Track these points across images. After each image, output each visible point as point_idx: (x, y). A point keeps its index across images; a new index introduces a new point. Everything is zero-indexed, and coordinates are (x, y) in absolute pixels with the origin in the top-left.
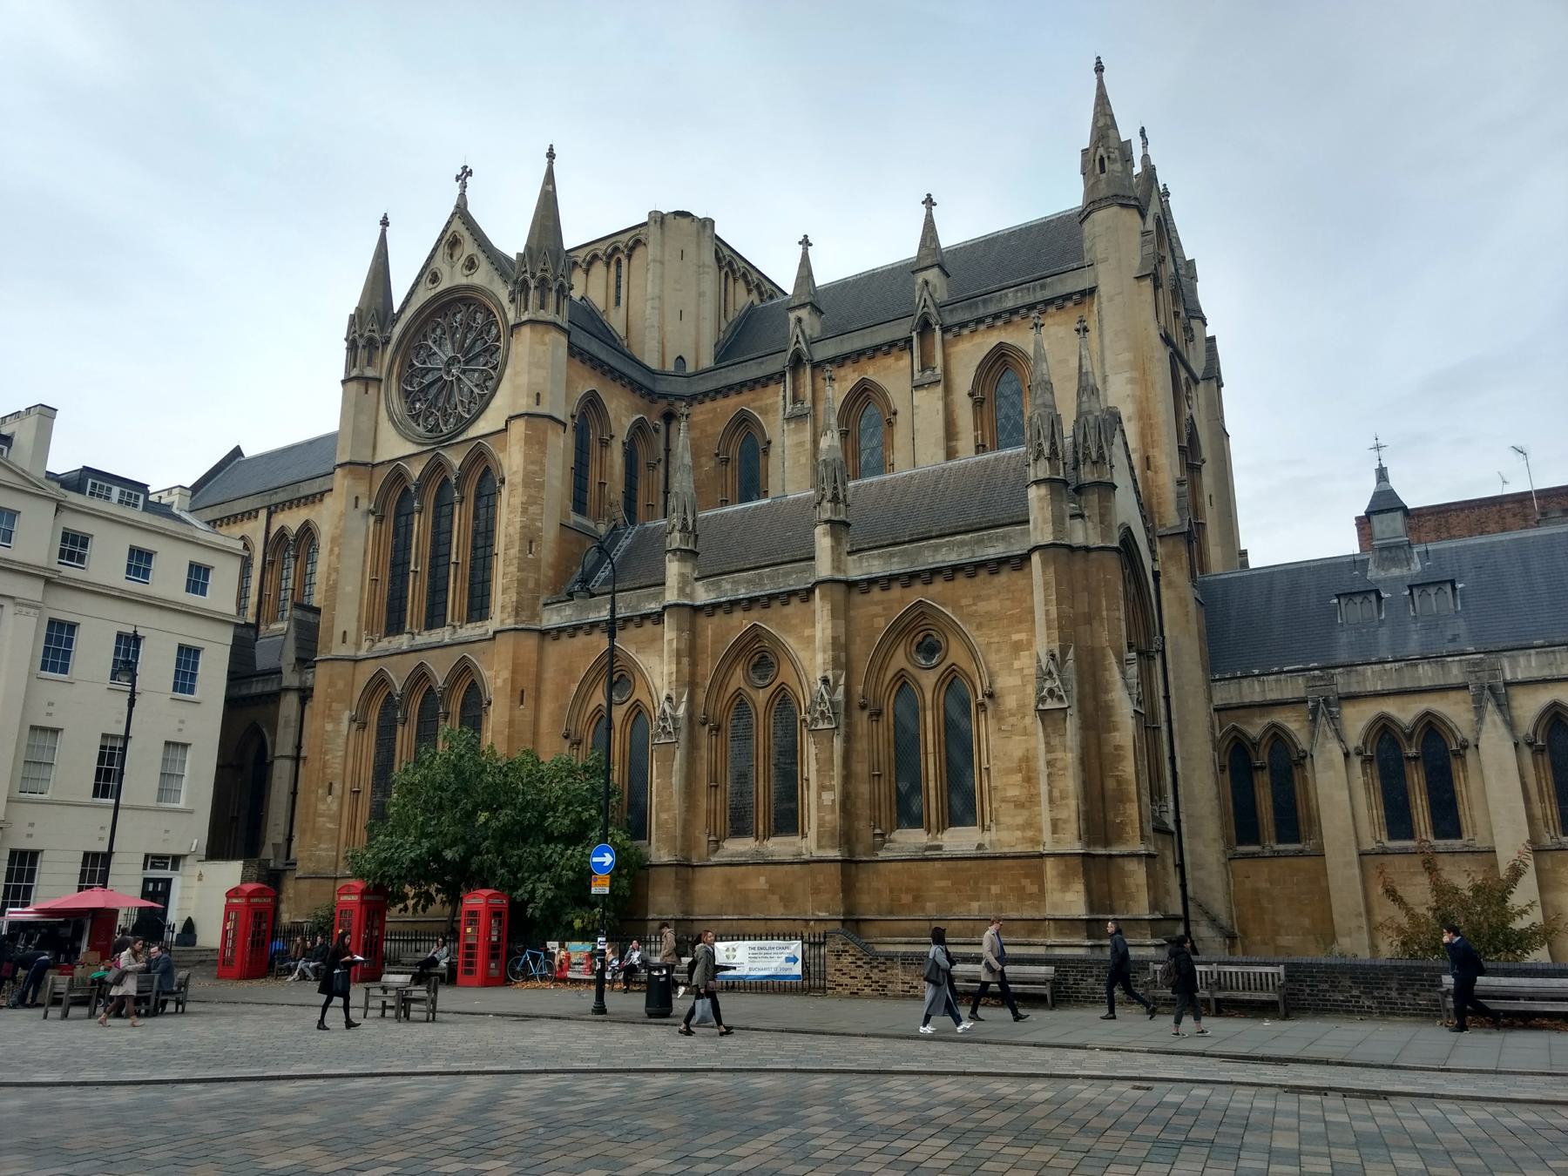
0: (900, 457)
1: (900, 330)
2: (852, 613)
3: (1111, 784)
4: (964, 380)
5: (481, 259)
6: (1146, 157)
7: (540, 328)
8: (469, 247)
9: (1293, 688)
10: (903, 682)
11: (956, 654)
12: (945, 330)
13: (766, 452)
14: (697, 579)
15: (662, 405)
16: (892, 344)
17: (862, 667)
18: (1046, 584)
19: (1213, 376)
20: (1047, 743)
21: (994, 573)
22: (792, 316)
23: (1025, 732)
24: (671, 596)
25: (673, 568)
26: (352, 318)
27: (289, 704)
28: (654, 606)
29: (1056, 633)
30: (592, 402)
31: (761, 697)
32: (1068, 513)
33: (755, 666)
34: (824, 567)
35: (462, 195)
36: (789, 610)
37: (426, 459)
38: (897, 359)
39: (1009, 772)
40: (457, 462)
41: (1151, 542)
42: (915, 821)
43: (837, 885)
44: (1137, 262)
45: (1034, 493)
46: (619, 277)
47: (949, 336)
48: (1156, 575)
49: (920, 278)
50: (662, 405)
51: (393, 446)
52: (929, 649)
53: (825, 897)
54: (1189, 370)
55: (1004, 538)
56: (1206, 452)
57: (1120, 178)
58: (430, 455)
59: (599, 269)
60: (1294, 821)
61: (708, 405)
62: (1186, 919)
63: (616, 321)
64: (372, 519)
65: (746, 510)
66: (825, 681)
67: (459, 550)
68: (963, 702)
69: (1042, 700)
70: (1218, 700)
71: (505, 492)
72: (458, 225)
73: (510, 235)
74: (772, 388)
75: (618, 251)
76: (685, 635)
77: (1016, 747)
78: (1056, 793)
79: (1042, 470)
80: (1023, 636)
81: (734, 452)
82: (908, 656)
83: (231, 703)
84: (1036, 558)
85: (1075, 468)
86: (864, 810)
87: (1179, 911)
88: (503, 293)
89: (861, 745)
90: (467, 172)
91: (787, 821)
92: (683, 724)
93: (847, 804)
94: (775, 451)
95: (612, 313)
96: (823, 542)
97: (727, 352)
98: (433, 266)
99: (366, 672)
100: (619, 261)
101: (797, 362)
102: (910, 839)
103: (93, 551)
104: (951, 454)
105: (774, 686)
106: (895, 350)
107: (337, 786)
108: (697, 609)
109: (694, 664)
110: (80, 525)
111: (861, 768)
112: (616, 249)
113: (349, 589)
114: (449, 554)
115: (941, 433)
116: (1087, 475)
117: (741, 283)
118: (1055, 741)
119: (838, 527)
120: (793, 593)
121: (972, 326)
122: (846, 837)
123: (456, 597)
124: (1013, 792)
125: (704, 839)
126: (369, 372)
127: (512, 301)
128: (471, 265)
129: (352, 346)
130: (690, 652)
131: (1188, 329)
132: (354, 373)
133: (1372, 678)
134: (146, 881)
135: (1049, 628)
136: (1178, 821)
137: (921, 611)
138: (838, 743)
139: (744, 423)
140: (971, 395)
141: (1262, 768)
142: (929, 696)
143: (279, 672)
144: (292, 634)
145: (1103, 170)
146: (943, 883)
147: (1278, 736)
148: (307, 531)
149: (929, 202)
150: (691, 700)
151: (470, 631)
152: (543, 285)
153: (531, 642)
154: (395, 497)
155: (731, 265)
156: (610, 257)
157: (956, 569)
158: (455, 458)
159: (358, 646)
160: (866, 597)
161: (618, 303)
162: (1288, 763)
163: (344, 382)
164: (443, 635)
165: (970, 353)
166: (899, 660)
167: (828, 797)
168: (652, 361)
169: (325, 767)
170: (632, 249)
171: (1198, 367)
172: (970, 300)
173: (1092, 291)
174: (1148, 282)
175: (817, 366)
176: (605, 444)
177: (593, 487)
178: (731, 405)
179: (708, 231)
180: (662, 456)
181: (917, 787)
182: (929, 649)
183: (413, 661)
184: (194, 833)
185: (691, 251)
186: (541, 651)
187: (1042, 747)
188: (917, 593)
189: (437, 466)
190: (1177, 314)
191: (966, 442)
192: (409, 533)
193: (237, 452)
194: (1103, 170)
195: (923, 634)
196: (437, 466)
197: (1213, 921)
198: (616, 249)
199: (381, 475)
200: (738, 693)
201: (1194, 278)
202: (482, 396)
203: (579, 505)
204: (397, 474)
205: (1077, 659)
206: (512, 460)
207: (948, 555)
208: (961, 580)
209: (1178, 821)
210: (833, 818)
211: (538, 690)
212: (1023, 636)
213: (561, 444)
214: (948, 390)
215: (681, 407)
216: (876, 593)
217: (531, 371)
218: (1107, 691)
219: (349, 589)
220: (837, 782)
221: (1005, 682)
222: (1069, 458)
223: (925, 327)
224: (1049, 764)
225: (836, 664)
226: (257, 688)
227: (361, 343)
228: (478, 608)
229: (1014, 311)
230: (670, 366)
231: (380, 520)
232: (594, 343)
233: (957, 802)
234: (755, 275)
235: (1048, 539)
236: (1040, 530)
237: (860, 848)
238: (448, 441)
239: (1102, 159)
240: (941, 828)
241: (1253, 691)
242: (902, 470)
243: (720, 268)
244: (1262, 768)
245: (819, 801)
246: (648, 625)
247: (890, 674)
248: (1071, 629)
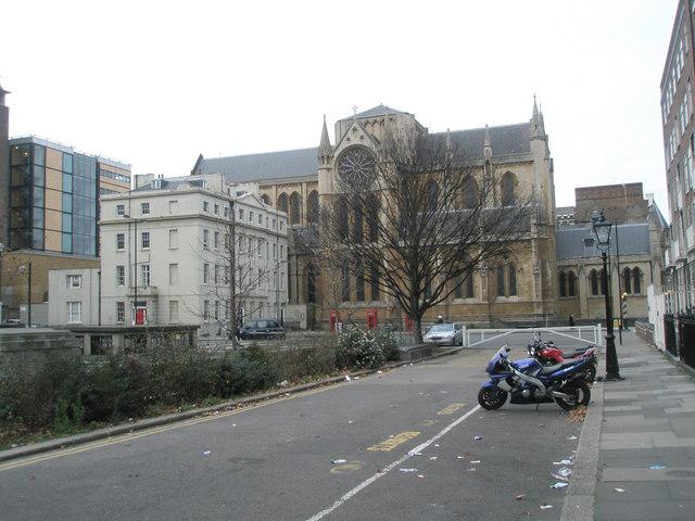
42: (502, 295)
60: (573, 291)
77: (527, 280)
91: (471, 294)
102: (502, 299)
147: (571, 274)
162: (572, 278)
196: (357, 197)
206: (386, 200)
221: (525, 266)
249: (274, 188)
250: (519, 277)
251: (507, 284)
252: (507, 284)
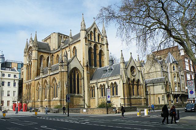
9: (95, 81)
15: (52, 54)
52: (56, 81)
62: (84, 105)
87: (84, 104)
90: (31, 34)
93: (49, 96)
102: (54, 98)
122: (49, 99)
126: (26, 55)
133: (100, 80)
134: (13, 103)
150: (42, 86)
173: (80, 40)
174: (85, 39)
197: (87, 105)
211: (35, 85)
214: (71, 51)
229: (75, 43)
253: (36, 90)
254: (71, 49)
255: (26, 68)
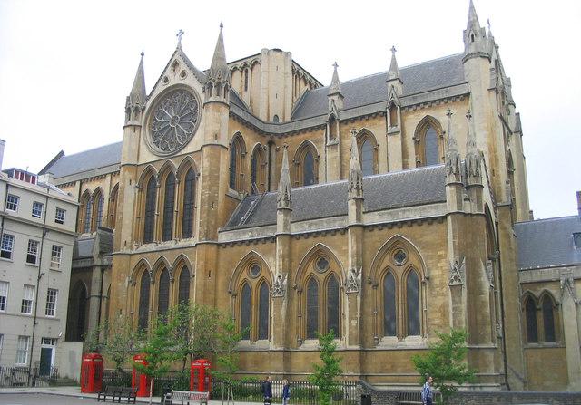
0: (381, 166)
1: (381, 108)
2: (366, 240)
3: (480, 318)
4: (411, 132)
5: (188, 71)
6: (490, 32)
7: (217, 105)
8: (183, 67)
10: (388, 272)
11: (413, 260)
12: (402, 109)
13: (317, 161)
14: (291, 222)
15: (268, 138)
16: (377, 114)
17: (369, 265)
18: (454, 230)
19: (519, 132)
20: (453, 300)
21: (430, 224)
22: (330, 99)
23: (443, 295)
24: (280, 230)
25: (280, 217)
26: (128, 97)
27: (97, 273)
28: (271, 234)
29: (458, 252)
30: (238, 138)
31: (321, 277)
32: (464, 198)
33: (319, 263)
34: (352, 219)
35: (179, 43)
36: (335, 238)
37: (164, 162)
38: (379, 121)
39: (436, 312)
40: (177, 166)
41: (495, 209)
42: (392, 333)
43: (358, 361)
44: (488, 83)
45: (448, 188)
46: (247, 77)
47: (404, 111)
48: (497, 224)
49: (390, 84)
50: (268, 138)
51: (147, 157)
53: (353, 366)
54: (508, 128)
55: (436, 208)
56: (515, 166)
57: (473, 32)
58: (165, 161)
59: (237, 74)
61: (289, 138)
63: (245, 98)
64: (137, 190)
65: (309, 191)
66: (353, 271)
67: (178, 205)
68: (415, 281)
69: (452, 281)
70: (522, 280)
71: (200, 179)
72: (177, 57)
73: (203, 62)
74: (320, 131)
75: (248, 66)
76: (287, 248)
77: (439, 302)
78: (457, 322)
79: (452, 179)
80: (442, 253)
81: (302, 160)
82: (391, 260)
83: (74, 271)
84: (449, 218)
85: (466, 178)
86: (370, 329)
88: (197, 87)
89: (369, 300)
92: (285, 288)
94: (322, 161)
95: (244, 93)
96: (352, 208)
97: (296, 113)
98: (166, 75)
99: (136, 260)
100: (247, 71)
101: (332, 119)
102: (390, 341)
103: (20, 203)
104: (405, 167)
105: (328, 272)
106: (378, 117)
107: (124, 310)
108: (292, 236)
109: (291, 261)
110: (12, 192)
111: (369, 310)
112: (246, 65)
113: (127, 222)
114: (173, 207)
115: (401, 155)
116: (472, 181)
117: (302, 82)
118: (457, 299)
119: (359, 201)
120: (338, 230)
121: (414, 107)
123: (177, 227)
124: (436, 321)
125: (295, 340)
126: (136, 123)
127: (204, 92)
128: (184, 74)
129: (128, 110)
130: (288, 257)
131: (508, 110)
132: (129, 123)
135: (455, 249)
136: (504, 333)
137: (397, 240)
138: (359, 299)
139: (306, 147)
140: (414, 138)
141: (540, 309)
142: (400, 278)
143: (91, 257)
144: (98, 241)
145: (473, 41)
146: (403, 360)
147: (547, 297)
148: (98, 192)
149: (394, 50)
151: (184, 243)
152: (218, 85)
153: (214, 248)
154: (148, 180)
155: (299, 74)
156: (242, 68)
157: (413, 222)
158: (176, 164)
159: (132, 248)
160: (372, 233)
161: (246, 90)
163: (124, 127)
164: (171, 244)
165: (413, 121)
166: (387, 262)
167: (354, 323)
168: (263, 117)
169: (118, 302)
170: (253, 66)
171: (512, 126)
172: (414, 96)
173: (468, 95)
174: (493, 93)
175: (341, 122)
176: (243, 156)
177: (238, 176)
178: (301, 138)
179: (289, 58)
180: (267, 161)
181: (393, 318)
182: (400, 257)
183: (158, 256)
184: (61, 332)
185: (281, 66)
186: (218, 253)
187: (451, 301)
188: (395, 232)
189: (168, 167)
190: (503, 103)
191: (412, 160)
192: (154, 197)
193: (62, 153)
194: (473, 41)
195: (398, 250)
198: (246, 65)
199: (141, 170)
200: (311, 275)
201: (510, 86)
202: (189, 135)
203: (232, 185)
204: (149, 171)
205: (467, 263)
206: (203, 166)
207: (411, 214)
208: (415, 227)
209: (504, 333)
210: (356, 332)
212: (442, 253)
213: (225, 159)
215: (276, 139)
216: (376, 231)
217: (213, 126)
218: (479, 277)
219: (127, 222)
220: (358, 316)
221: (435, 273)
222: (463, 174)
223: (393, 106)
224: (453, 309)
225: (358, 264)
226: (81, 264)
227: (132, 109)
228: (187, 232)
230: (271, 120)
231: (141, 190)
232: (241, 113)
233: (411, 325)
234: (309, 77)
235: (455, 210)
236: (451, 206)
237: (368, 344)
238: (173, 156)
239: (472, 36)
240: (404, 336)
241: (536, 276)
242: (382, 174)
243: (293, 74)
244: (540, 309)
245: (348, 324)
246: (268, 243)
247: (383, 267)
248: (464, 251)
249: (109, 177)
250: (424, 293)
251: (400, 310)
252: (400, 310)
253: (222, 295)
254: (403, 127)
255: (134, 184)
